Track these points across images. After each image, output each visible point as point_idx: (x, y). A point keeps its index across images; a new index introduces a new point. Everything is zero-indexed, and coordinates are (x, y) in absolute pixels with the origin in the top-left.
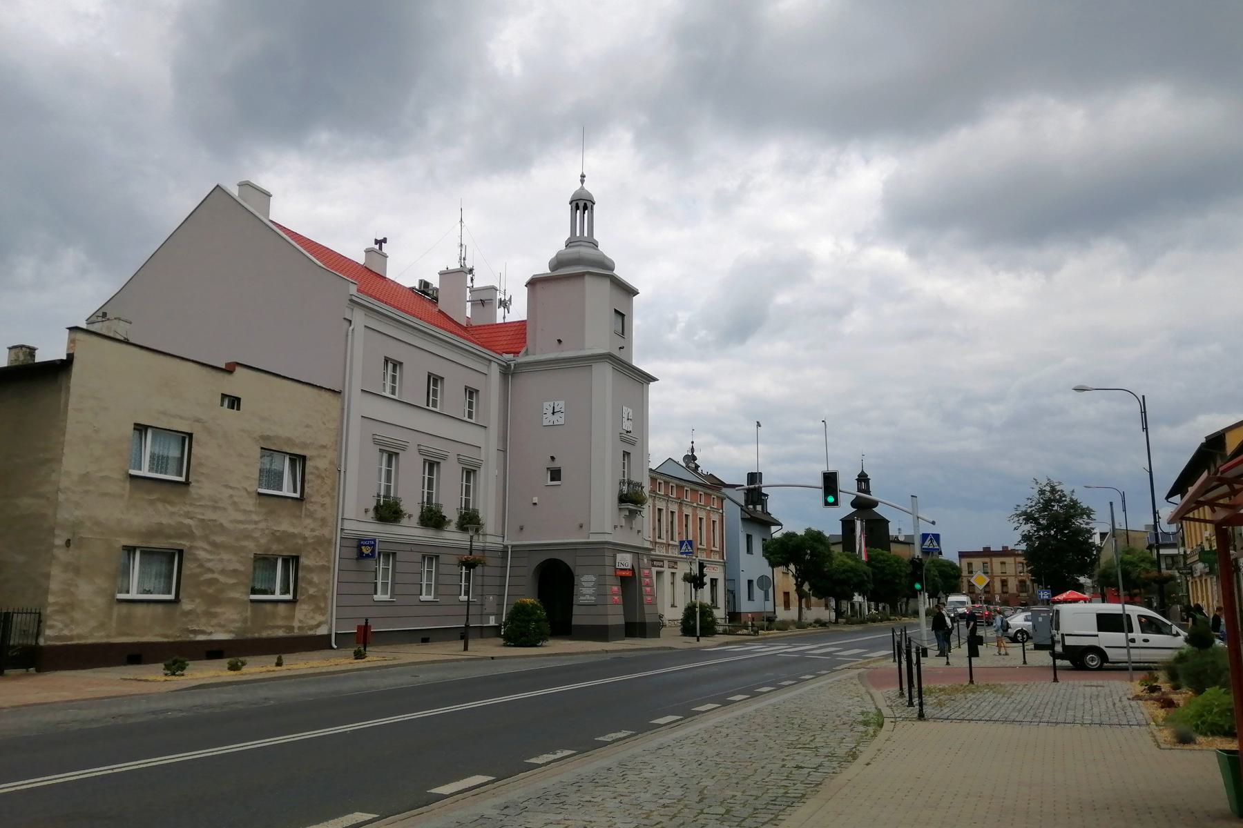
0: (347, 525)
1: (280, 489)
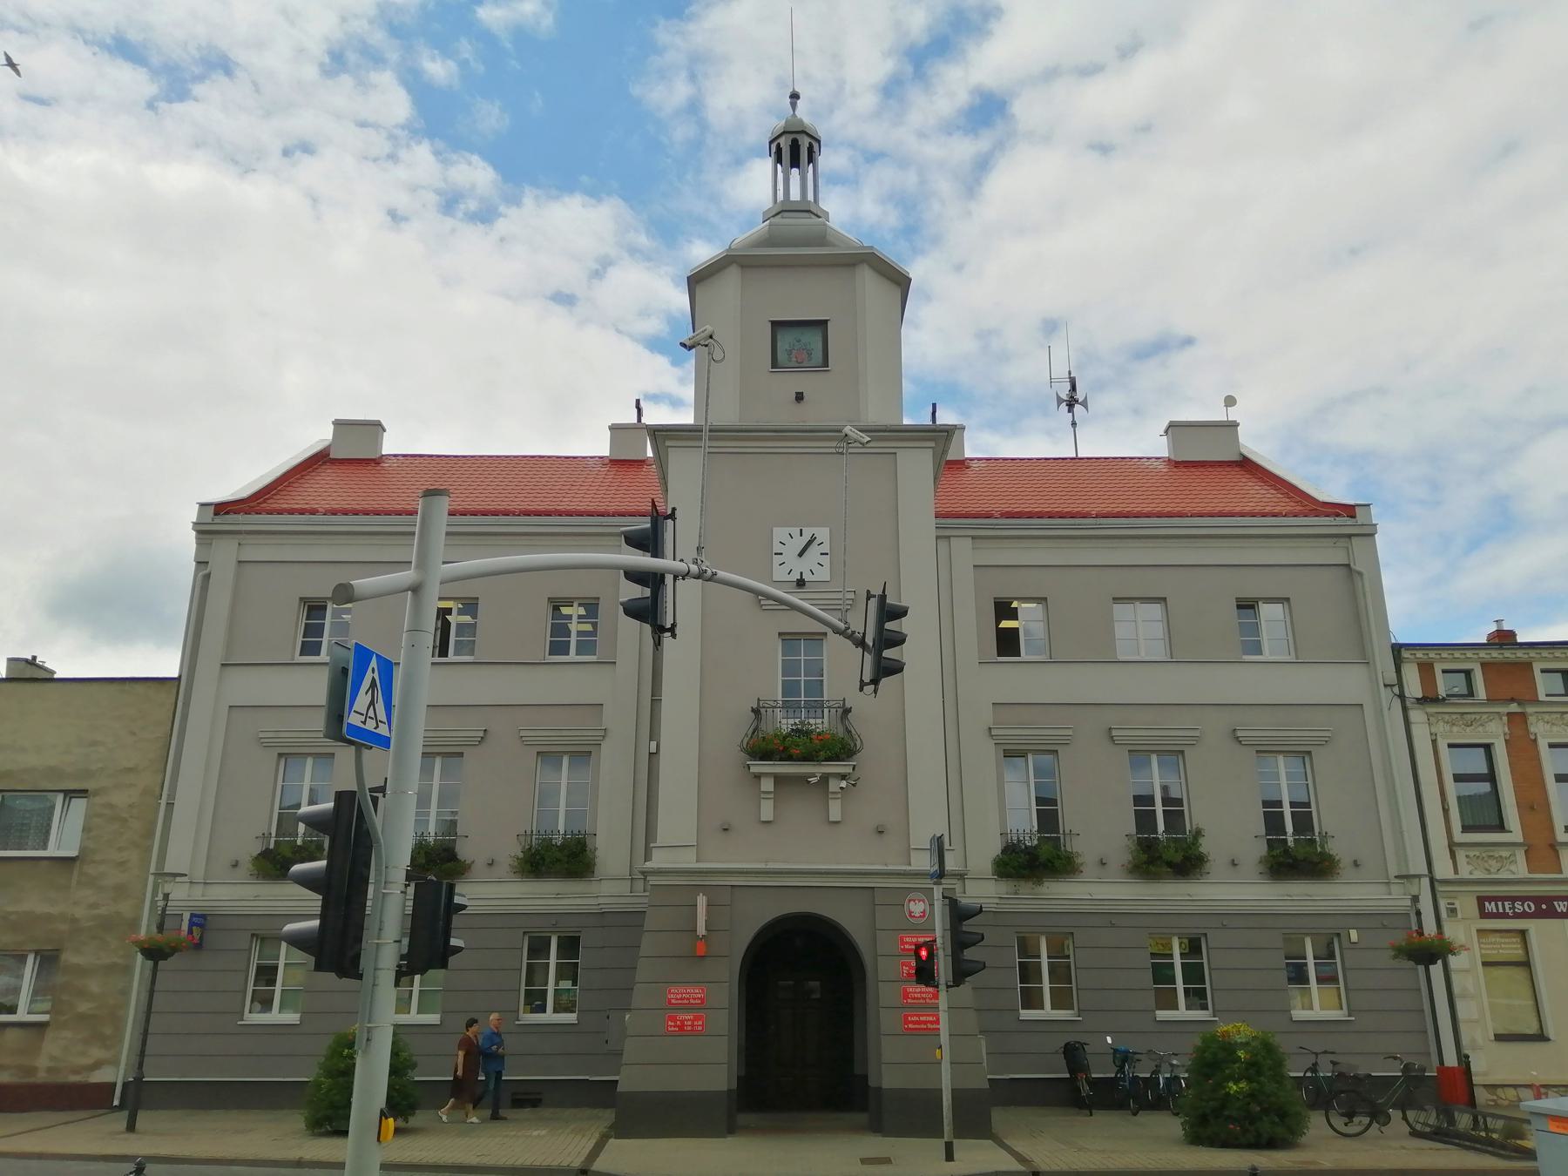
1: (45, 847)
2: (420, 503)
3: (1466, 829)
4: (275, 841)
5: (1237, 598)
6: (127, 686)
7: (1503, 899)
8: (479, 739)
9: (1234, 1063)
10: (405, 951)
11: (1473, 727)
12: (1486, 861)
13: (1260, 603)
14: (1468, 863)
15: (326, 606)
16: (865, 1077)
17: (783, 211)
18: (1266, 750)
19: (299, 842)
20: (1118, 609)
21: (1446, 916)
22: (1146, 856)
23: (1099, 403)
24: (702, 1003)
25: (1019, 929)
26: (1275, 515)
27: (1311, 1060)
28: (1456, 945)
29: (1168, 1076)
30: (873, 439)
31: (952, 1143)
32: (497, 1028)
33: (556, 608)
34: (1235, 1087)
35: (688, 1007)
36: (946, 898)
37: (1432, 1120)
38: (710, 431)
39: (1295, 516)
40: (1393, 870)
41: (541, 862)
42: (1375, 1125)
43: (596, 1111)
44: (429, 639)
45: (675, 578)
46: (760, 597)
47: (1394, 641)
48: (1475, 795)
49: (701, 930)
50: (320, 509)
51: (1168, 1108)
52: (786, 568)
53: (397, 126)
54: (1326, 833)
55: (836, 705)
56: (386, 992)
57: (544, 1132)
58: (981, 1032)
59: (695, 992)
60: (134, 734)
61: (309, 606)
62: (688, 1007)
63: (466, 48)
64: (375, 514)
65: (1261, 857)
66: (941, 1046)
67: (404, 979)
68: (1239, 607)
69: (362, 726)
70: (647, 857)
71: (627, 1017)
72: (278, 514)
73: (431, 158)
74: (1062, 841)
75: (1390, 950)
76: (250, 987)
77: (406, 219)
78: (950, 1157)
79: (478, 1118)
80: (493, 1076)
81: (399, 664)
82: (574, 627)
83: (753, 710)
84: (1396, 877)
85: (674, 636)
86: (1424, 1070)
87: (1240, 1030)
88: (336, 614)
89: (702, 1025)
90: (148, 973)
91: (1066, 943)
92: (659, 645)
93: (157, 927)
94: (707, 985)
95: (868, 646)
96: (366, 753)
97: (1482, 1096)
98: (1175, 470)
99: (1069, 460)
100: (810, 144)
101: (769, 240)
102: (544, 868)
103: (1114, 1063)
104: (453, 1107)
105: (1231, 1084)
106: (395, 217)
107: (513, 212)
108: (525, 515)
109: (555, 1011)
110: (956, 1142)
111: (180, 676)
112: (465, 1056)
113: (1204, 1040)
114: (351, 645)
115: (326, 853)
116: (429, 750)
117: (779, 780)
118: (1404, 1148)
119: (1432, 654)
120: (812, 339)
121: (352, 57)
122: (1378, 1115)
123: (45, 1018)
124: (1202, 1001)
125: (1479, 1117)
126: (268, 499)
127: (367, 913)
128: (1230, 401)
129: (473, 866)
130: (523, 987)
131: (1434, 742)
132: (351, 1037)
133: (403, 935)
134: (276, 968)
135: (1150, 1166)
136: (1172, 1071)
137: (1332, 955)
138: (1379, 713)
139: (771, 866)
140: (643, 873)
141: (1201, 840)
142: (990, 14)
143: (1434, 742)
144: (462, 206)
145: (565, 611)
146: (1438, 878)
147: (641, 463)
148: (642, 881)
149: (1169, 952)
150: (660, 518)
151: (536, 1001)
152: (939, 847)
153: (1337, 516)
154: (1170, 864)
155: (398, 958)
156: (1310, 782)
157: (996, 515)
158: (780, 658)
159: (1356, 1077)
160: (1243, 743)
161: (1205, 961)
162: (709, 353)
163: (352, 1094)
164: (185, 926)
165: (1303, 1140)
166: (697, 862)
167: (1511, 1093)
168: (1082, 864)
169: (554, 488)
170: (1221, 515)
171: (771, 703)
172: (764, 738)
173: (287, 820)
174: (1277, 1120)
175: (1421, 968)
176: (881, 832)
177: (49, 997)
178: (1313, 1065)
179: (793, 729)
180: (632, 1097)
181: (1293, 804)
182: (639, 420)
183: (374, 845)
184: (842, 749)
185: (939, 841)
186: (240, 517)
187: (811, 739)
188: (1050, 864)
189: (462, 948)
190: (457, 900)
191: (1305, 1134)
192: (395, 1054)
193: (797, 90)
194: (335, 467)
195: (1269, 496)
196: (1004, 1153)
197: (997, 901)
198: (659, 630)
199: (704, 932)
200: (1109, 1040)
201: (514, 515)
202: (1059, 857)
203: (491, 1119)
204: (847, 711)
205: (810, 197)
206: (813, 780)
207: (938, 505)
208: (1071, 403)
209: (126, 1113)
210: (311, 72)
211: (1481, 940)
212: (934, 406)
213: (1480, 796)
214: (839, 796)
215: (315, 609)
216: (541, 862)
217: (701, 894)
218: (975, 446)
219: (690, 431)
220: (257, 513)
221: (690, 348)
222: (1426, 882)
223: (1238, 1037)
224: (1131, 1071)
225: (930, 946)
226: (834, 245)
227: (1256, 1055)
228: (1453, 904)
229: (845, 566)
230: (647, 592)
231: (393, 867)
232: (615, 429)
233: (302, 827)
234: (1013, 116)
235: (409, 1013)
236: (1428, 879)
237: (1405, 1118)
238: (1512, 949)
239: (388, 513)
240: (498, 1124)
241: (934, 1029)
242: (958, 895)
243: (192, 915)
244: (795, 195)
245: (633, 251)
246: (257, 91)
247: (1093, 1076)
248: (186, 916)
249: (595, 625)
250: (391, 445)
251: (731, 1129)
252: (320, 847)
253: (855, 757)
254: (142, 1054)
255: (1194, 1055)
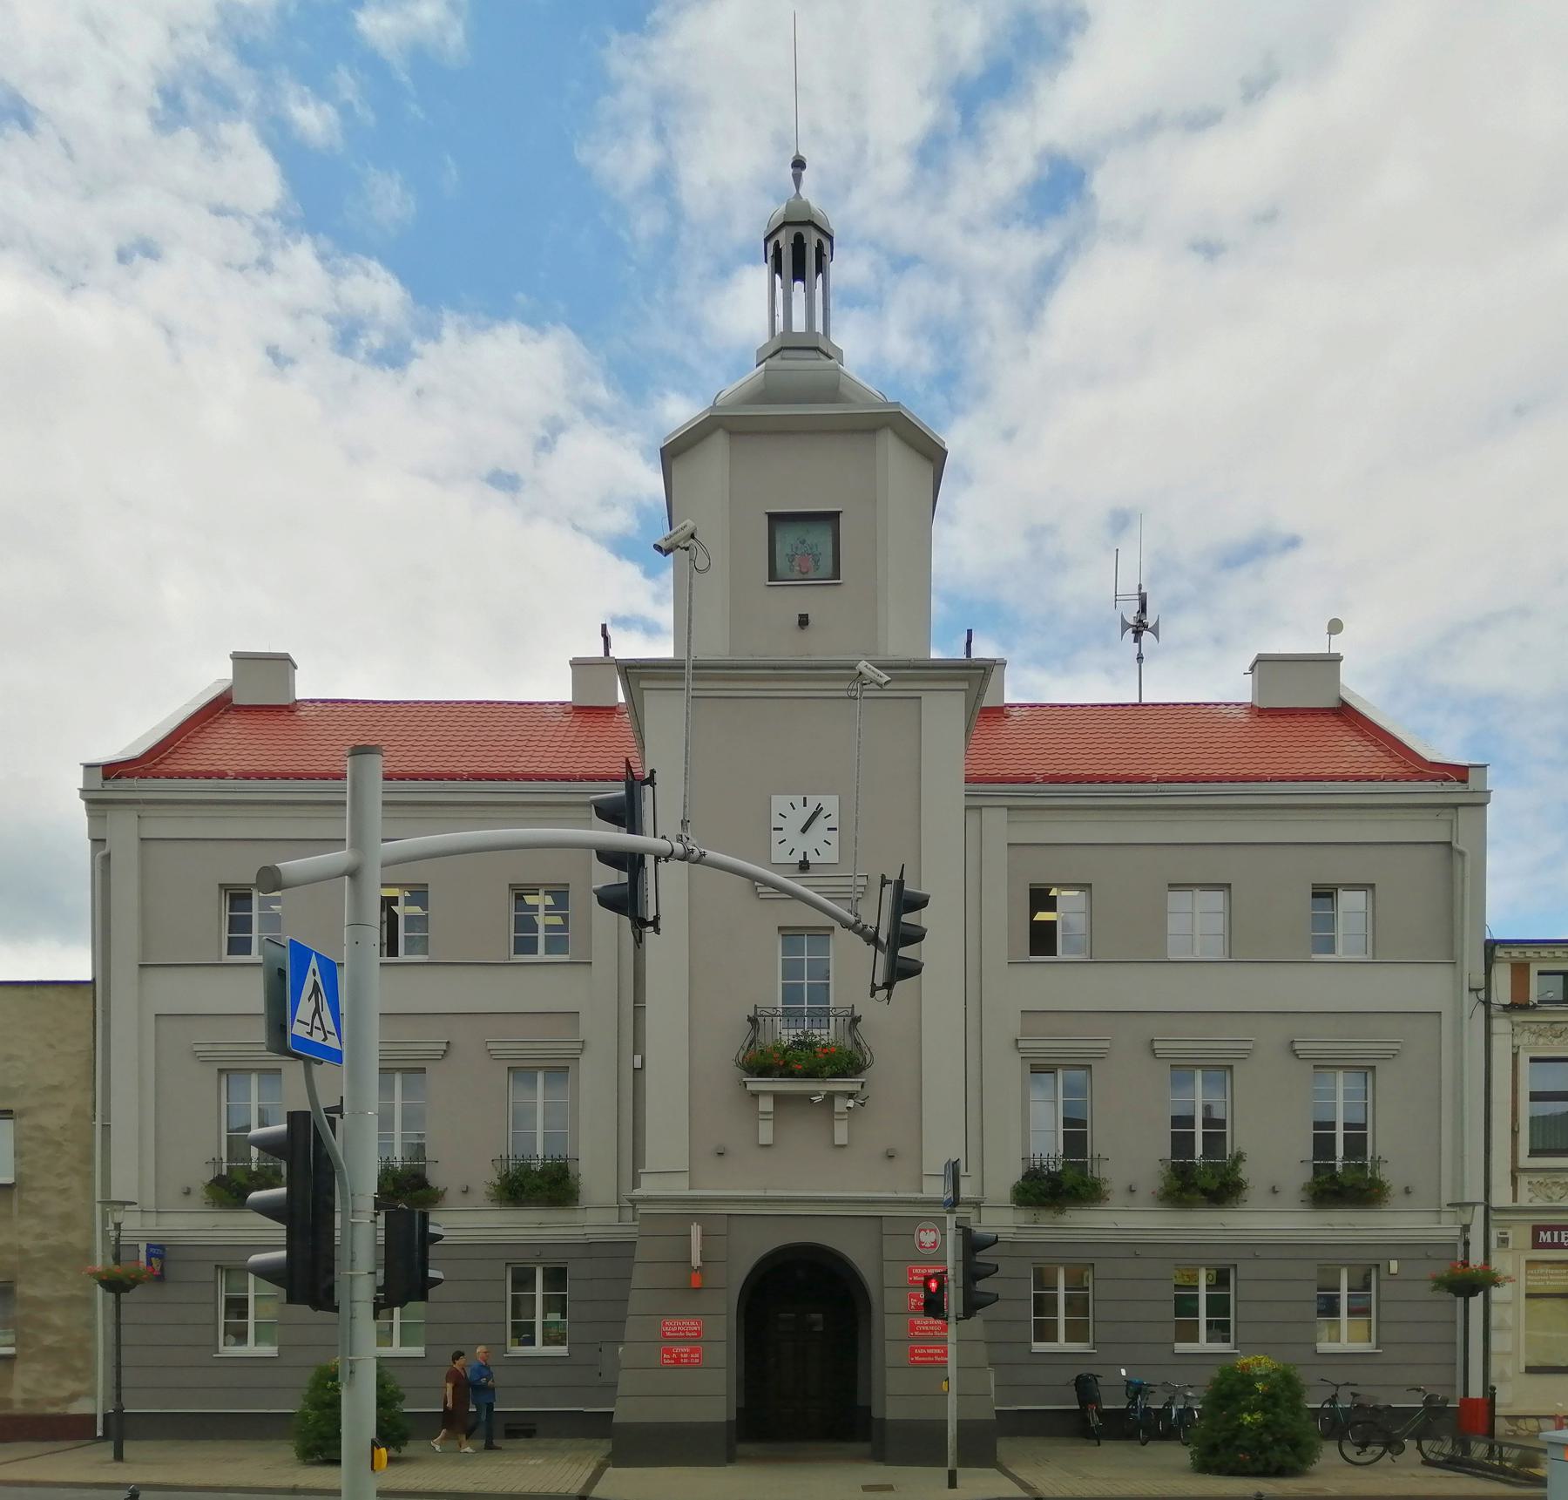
0: (133, 1224)
2: (348, 763)
3: (1534, 1153)
4: (228, 1167)
5: (1313, 884)
6: (36, 991)
8: (442, 1053)
9: (1251, 1395)
10: (381, 1282)
11: (1562, 1039)
12: (1550, 1188)
13: (1340, 891)
14: (1529, 1190)
15: (251, 894)
16: (869, 1409)
17: (783, 348)
18: (1322, 1066)
19: (254, 1167)
20: (1174, 897)
21: (1496, 1247)
22: (1180, 1182)
23: (1176, 627)
24: (699, 1335)
25: (1036, 1260)
26: (1371, 779)
27: (1330, 1392)
28: (1501, 1277)
29: (1182, 1407)
30: (894, 678)
31: (955, 1471)
32: (485, 1361)
33: (519, 897)
34: (1249, 1419)
35: (685, 1340)
36: (960, 1227)
37: (1447, 1450)
38: (694, 668)
39: (1395, 781)
40: (1447, 1198)
41: (520, 1190)
42: (1388, 1454)
43: (592, 1441)
44: (374, 934)
45: (657, 859)
46: (756, 884)
47: (1488, 937)
48: (1550, 1116)
49: (696, 1260)
50: (229, 772)
51: (1178, 1438)
52: (787, 847)
53: (265, 214)
54: (1380, 1158)
55: (844, 1014)
56: (365, 1325)
57: (540, 1462)
58: (991, 1365)
59: (691, 1325)
60: (52, 1046)
61: (230, 894)
62: (685, 1340)
63: (346, 82)
64: (296, 779)
65: (1305, 1184)
66: (948, 1379)
67: (383, 1312)
68: (1315, 895)
69: (308, 1037)
70: (636, 1184)
71: (620, 1349)
72: (180, 778)
73: (315, 266)
74: (1089, 1166)
75: (1430, 1282)
76: (222, 1320)
77: (291, 361)
78: (952, 1484)
79: (471, 1448)
80: (485, 1407)
81: (343, 964)
82: (541, 920)
83: (749, 1019)
84: (1448, 1205)
85: (657, 931)
86: (1447, 1401)
87: (1261, 1363)
88: (264, 904)
89: (699, 1358)
90: (111, 1306)
91: (1086, 1274)
92: (641, 941)
93: (114, 1259)
94: (703, 1317)
95: (881, 943)
96: (316, 1068)
97: (1501, 1426)
98: (1258, 720)
99: (1131, 707)
100: (820, 242)
101: (764, 394)
102: (523, 1196)
103: (1127, 1394)
104: (446, 1438)
105: (1245, 1415)
106: (278, 357)
107: (429, 349)
108: (475, 779)
109: (545, 1343)
110: (959, 1470)
111: (94, 980)
112: (453, 1388)
113: (1222, 1372)
114: (285, 940)
115: (284, 1179)
116: (387, 1065)
117: (779, 1098)
118: (1414, 1476)
119: (1530, 953)
120: (819, 538)
121: (192, 99)
122: (1393, 1445)
123: (11, 1351)
124: (1225, 1334)
125: (1495, 1447)
126: (165, 758)
127: (336, 1243)
128: (1335, 627)
129: (446, 1194)
130: (509, 1321)
131: (1515, 1056)
132: (333, 1370)
133: (378, 1266)
134: (246, 1300)
135: (1154, 1493)
136: (1186, 1403)
137: (1367, 1287)
138: (1458, 1023)
139: (771, 1193)
140: (631, 1201)
141: (1242, 1166)
142: (1072, 22)
143: (1515, 1056)
144: (363, 341)
145: (530, 900)
146: (1493, 1206)
147: (611, 710)
148: (631, 1210)
149: (1196, 1284)
150: (637, 783)
151: (524, 1334)
152: (954, 1173)
153: (1445, 780)
154: (1204, 1191)
155: (375, 1290)
156: (1369, 1101)
157: (1038, 778)
158: (780, 957)
159: (1375, 1408)
160: (1300, 1056)
161: (1232, 1293)
162: (691, 560)
163: (340, 1425)
164: (143, 1257)
165: (1313, 1468)
166: (690, 1189)
167: (1532, 1424)
168: (1109, 1191)
169: (508, 744)
170: (1307, 778)
171: (770, 1011)
172: (762, 1051)
173: (237, 1143)
174: (1288, 1449)
175: (1460, 1300)
176: (891, 1157)
177: (10, 1330)
178: (1332, 1396)
179: (794, 1041)
180: (627, 1428)
181: (1347, 1126)
182: (607, 653)
183: (336, 1171)
184: (849, 1064)
185: (955, 1166)
186: (135, 783)
187: (815, 1052)
188: (1074, 1192)
189: (442, 1280)
190: (432, 1229)
191: (1315, 1462)
192: (381, 1386)
193: (801, 154)
194: (241, 717)
195: (1367, 754)
196: (1007, 1480)
197: (1014, 1230)
198: (640, 923)
199: (699, 1264)
200: (1123, 1372)
201: (462, 779)
202: (1084, 1184)
203: (485, 1449)
204: (856, 1020)
205: (819, 328)
206: (817, 1099)
207: (968, 761)
208: (1139, 629)
209: (111, 1444)
210: (138, 124)
211: (1528, 1272)
212: (970, 632)
213: (1556, 1116)
214: (846, 1117)
215: (238, 898)
216: (520, 1190)
217: (695, 1224)
218: (1019, 687)
219: (670, 668)
220: (154, 777)
221: (667, 552)
222: (1480, 1210)
223: (1257, 1369)
224: (1143, 1402)
225: (941, 1278)
226: (849, 401)
227: (1275, 1387)
228: (1506, 1234)
229: (856, 846)
230: (624, 877)
231: (360, 1195)
232: (577, 664)
233: (254, 1152)
234: (1093, 196)
235: (391, 1346)
236: (1483, 1207)
237: (1419, 1448)
238: (1558, 1280)
239: (311, 777)
240: (493, 1453)
241: (942, 1362)
242: (972, 1224)
243: (149, 1246)
244: (799, 324)
245: (590, 409)
246: (70, 156)
247: (1104, 1407)
248: (143, 1247)
249: (565, 918)
250: (305, 687)
251: (730, 1458)
252: (277, 1173)
253: (864, 1073)
254: (118, 1386)
255: (1211, 1387)
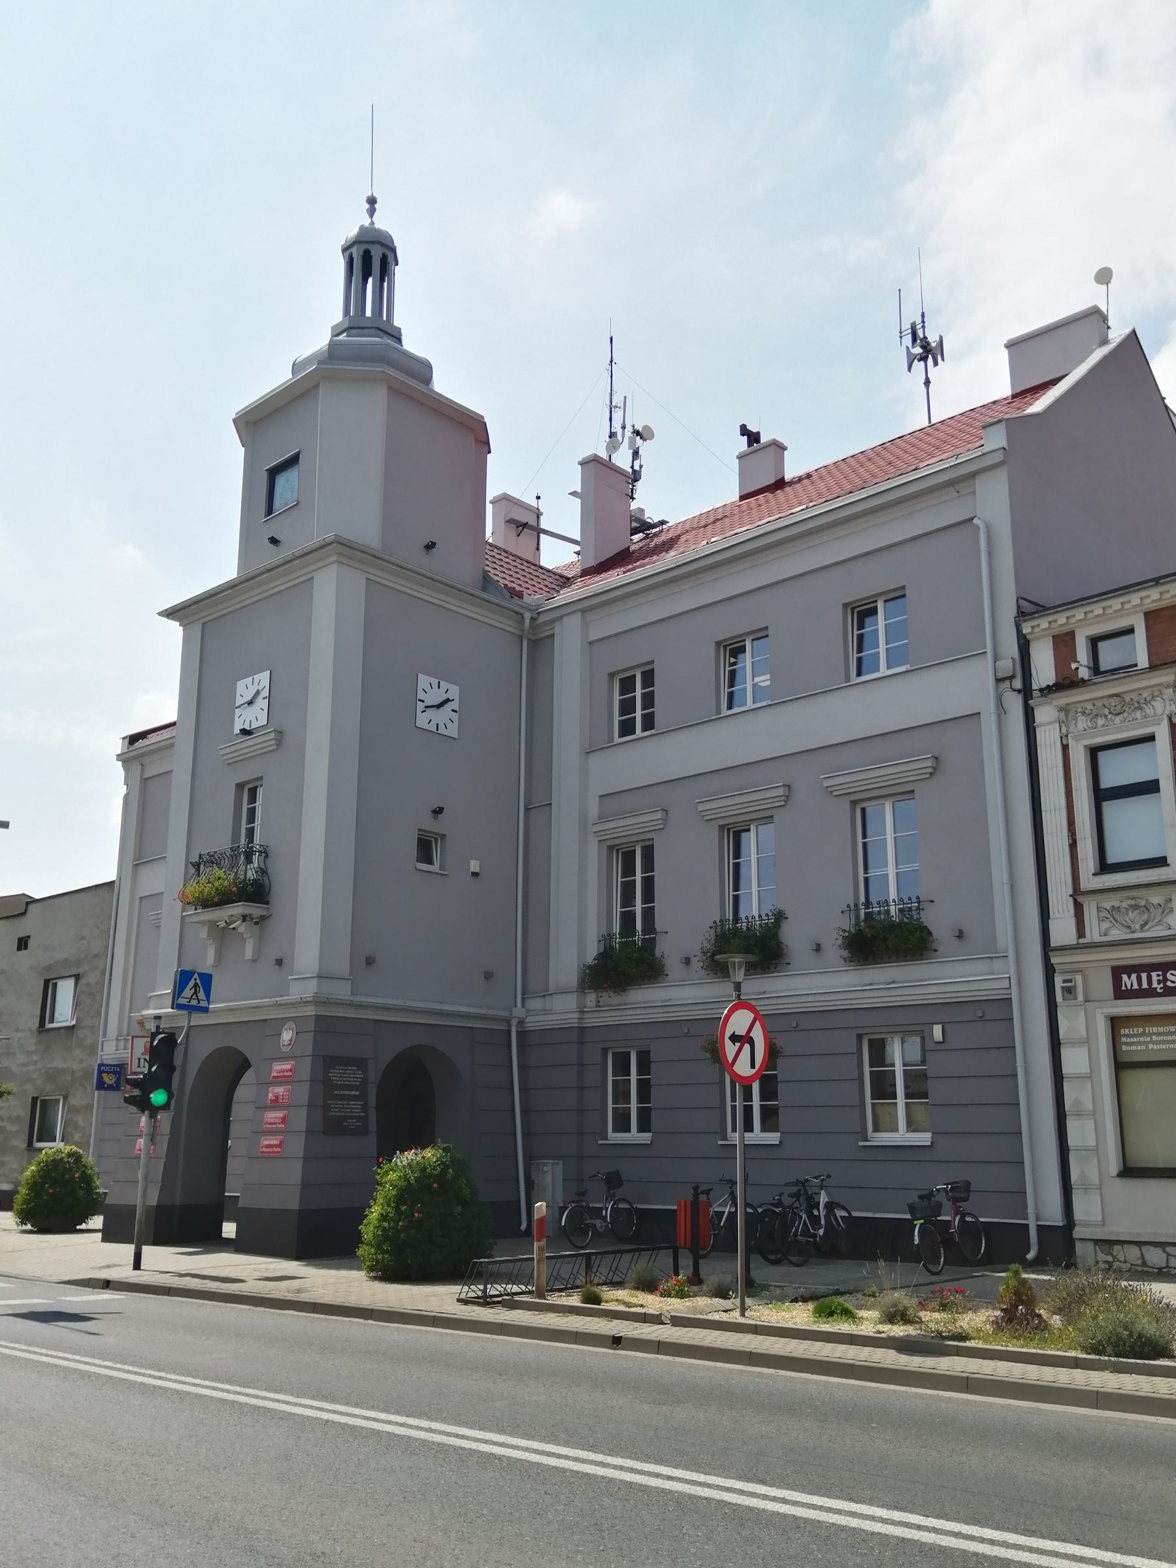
7: (1149, 968)
21: (1061, 1000)
228: (1070, 981)
